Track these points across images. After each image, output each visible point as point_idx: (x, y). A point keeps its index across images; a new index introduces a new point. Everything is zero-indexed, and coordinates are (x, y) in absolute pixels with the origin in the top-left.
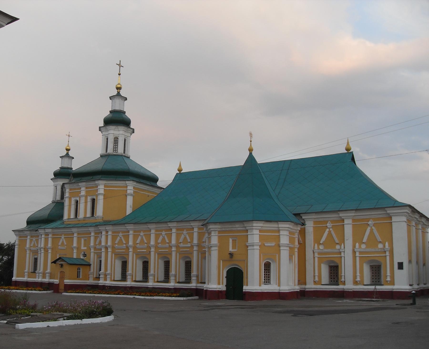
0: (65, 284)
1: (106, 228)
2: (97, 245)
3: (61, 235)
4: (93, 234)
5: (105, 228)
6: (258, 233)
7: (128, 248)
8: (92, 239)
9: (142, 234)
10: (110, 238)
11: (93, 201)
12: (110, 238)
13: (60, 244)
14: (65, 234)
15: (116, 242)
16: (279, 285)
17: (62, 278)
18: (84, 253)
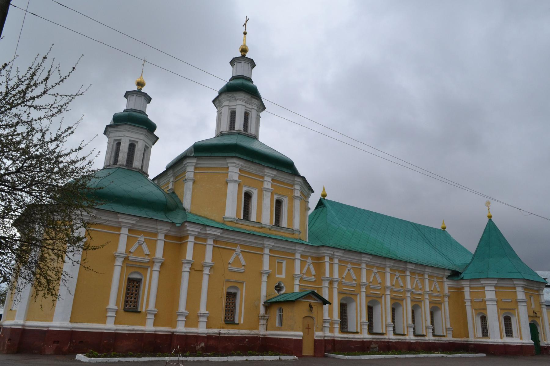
0: (316, 338)
1: (334, 252)
2: (304, 274)
3: (236, 245)
4: (298, 256)
5: (332, 253)
6: (494, 290)
7: (360, 285)
8: (298, 264)
9: (350, 266)
10: (336, 267)
11: (279, 203)
12: (336, 267)
13: (231, 261)
14: (242, 246)
15: (344, 276)
16: (521, 338)
17: (308, 329)
18: (279, 284)
